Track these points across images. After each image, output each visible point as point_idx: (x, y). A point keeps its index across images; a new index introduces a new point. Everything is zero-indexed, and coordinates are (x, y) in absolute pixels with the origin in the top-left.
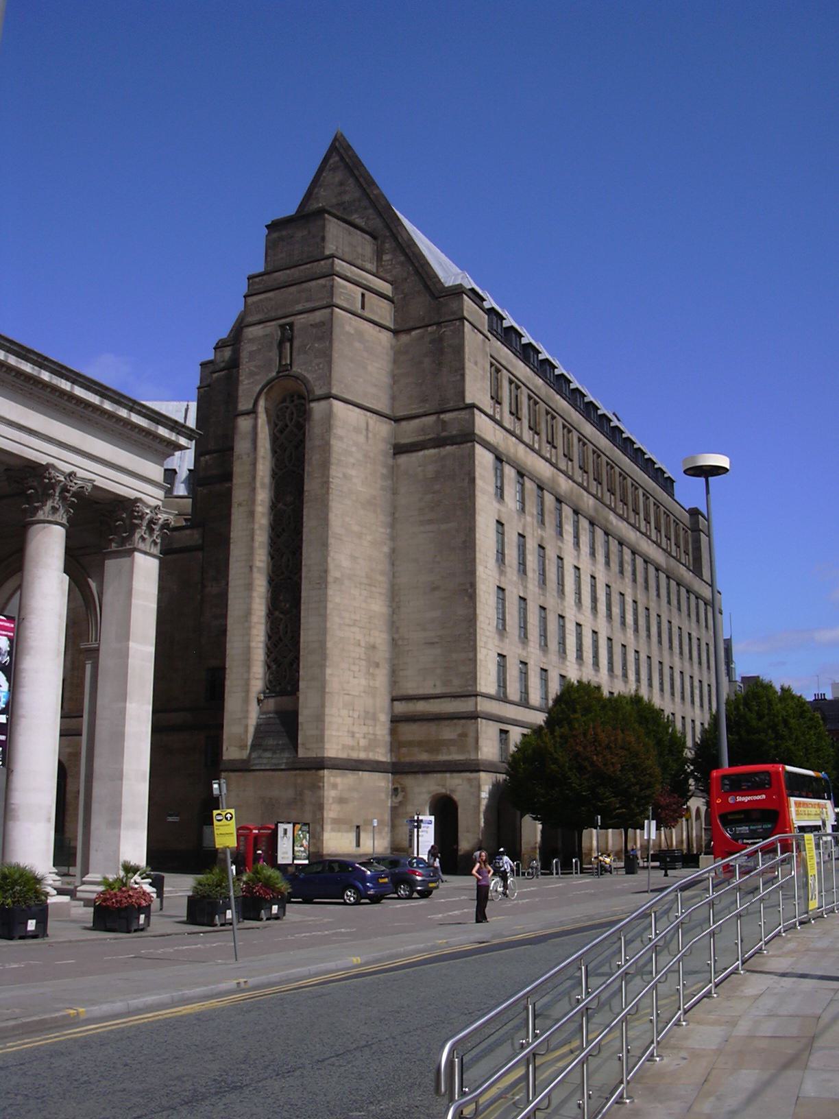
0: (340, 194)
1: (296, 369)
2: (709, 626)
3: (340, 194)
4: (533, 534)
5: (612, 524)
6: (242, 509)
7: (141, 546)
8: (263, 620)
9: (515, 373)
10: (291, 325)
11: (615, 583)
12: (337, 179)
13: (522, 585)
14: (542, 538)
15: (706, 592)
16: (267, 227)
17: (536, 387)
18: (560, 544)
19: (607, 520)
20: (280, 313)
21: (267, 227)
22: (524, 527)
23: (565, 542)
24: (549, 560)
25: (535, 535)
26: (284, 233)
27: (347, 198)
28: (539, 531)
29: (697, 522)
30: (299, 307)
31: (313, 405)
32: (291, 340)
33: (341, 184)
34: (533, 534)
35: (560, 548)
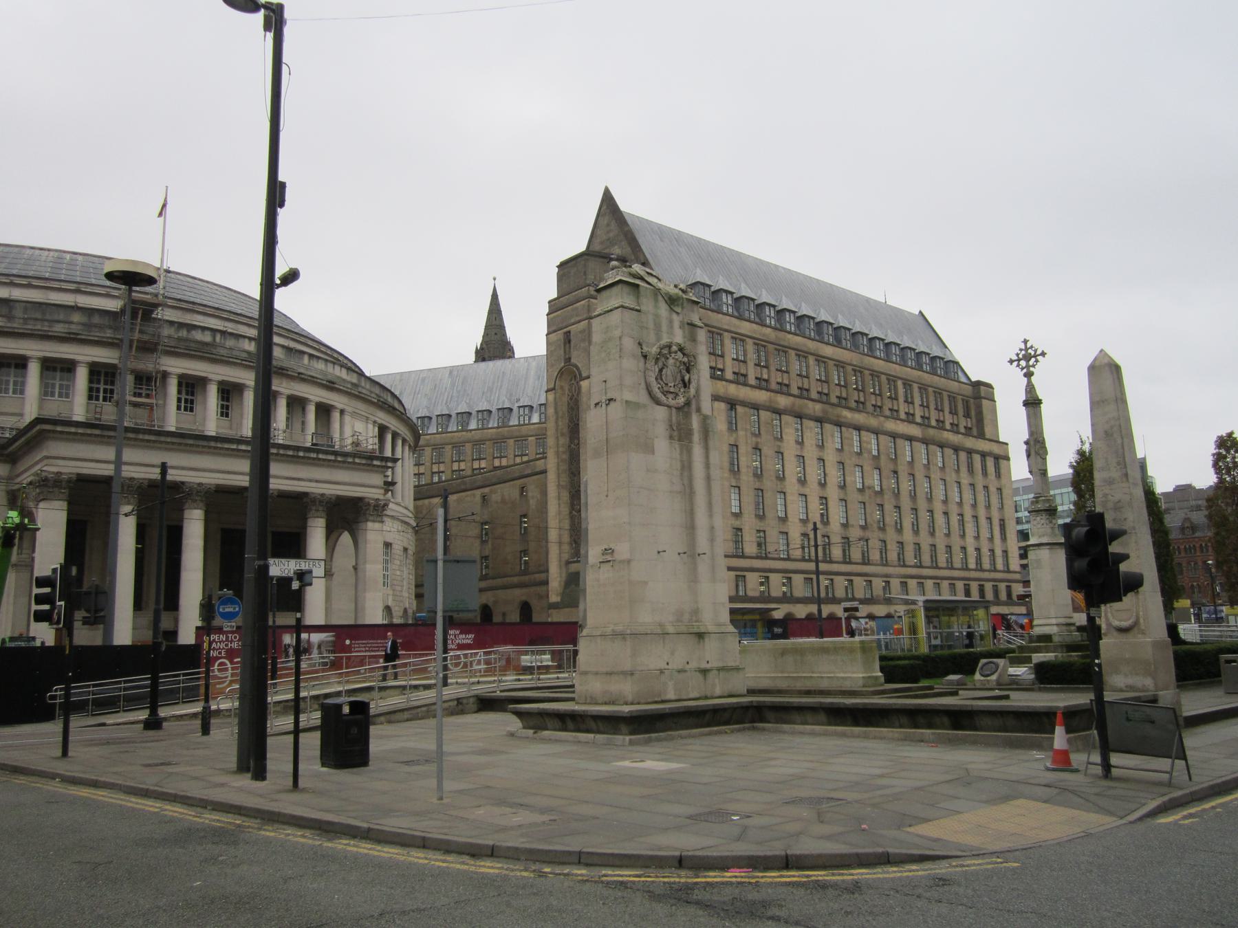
0: (608, 232)
1: (572, 361)
2: (989, 472)
3: (608, 232)
4: (747, 443)
5: (845, 417)
6: (552, 450)
7: (371, 518)
8: (567, 517)
9: (739, 331)
10: (569, 332)
11: (850, 459)
12: (606, 222)
13: (734, 478)
14: (757, 443)
15: (995, 449)
16: (558, 267)
17: (764, 335)
18: (779, 443)
19: (838, 416)
20: (564, 325)
21: (558, 267)
22: (736, 440)
23: (785, 441)
24: (766, 457)
25: (749, 441)
26: (566, 271)
27: (611, 235)
28: (754, 439)
29: (979, 392)
30: (573, 321)
31: (582, 383)
32: (569, 342)
33: (608, 225)
34: (747, 443)
35: (779, 447)
